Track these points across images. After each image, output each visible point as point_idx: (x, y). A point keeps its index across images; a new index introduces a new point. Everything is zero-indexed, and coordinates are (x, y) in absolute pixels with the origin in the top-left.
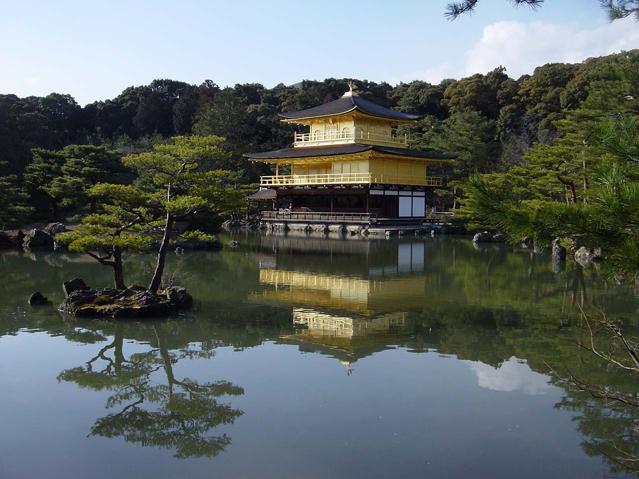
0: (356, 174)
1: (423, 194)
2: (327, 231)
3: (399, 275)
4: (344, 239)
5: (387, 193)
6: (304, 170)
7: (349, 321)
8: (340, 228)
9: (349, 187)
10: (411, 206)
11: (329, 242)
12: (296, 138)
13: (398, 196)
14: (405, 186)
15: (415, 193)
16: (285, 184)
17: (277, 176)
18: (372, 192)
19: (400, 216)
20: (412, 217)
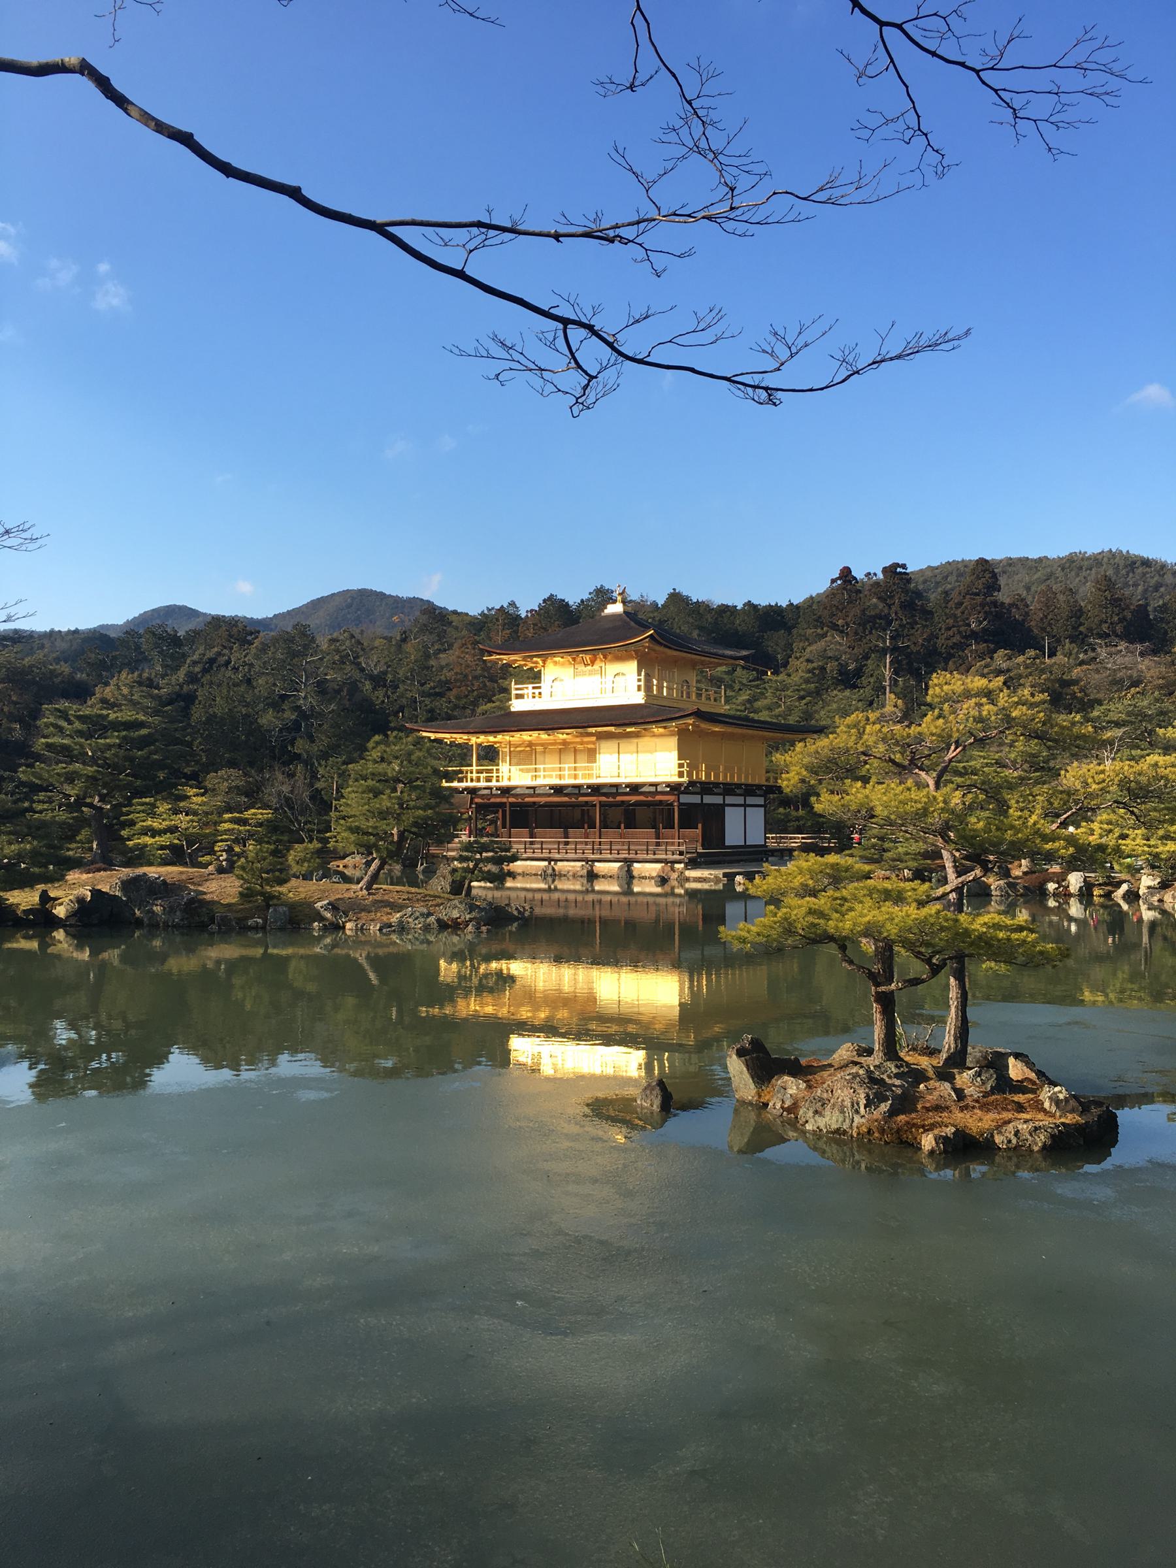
0: (653, 762)
1: (761, 801)
2: (592, 876)
3: (730, 960)
4: (628, 892)
5: (708, 799)
6: (527, 755)
7: (637, 1057)
8: (620, 868)
9: (635, 788)
10: (743, 825)
11: (632, 899)
12: (514, 692)
13: (724, 805)
14: (739, 786)
15: (751, 800)
16: (494, 783)
17: (474, 768)
18: (685, 799)
19: (727, 844)
20: (745, 846)
